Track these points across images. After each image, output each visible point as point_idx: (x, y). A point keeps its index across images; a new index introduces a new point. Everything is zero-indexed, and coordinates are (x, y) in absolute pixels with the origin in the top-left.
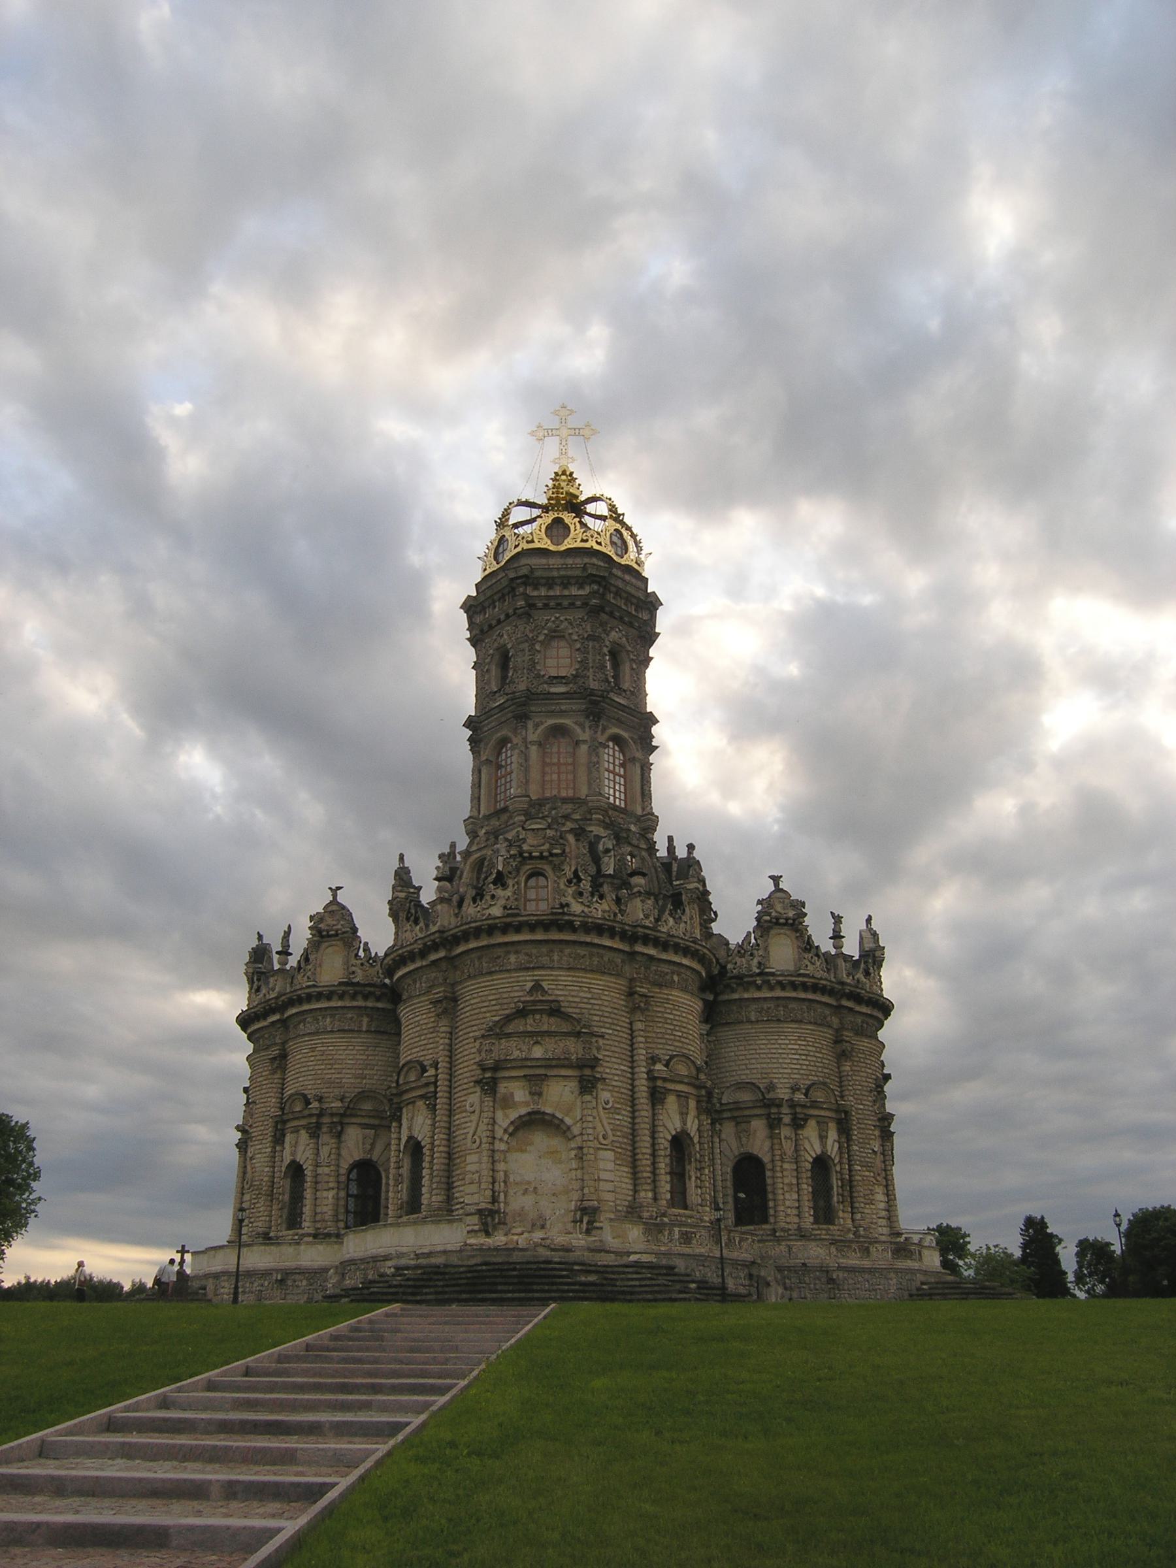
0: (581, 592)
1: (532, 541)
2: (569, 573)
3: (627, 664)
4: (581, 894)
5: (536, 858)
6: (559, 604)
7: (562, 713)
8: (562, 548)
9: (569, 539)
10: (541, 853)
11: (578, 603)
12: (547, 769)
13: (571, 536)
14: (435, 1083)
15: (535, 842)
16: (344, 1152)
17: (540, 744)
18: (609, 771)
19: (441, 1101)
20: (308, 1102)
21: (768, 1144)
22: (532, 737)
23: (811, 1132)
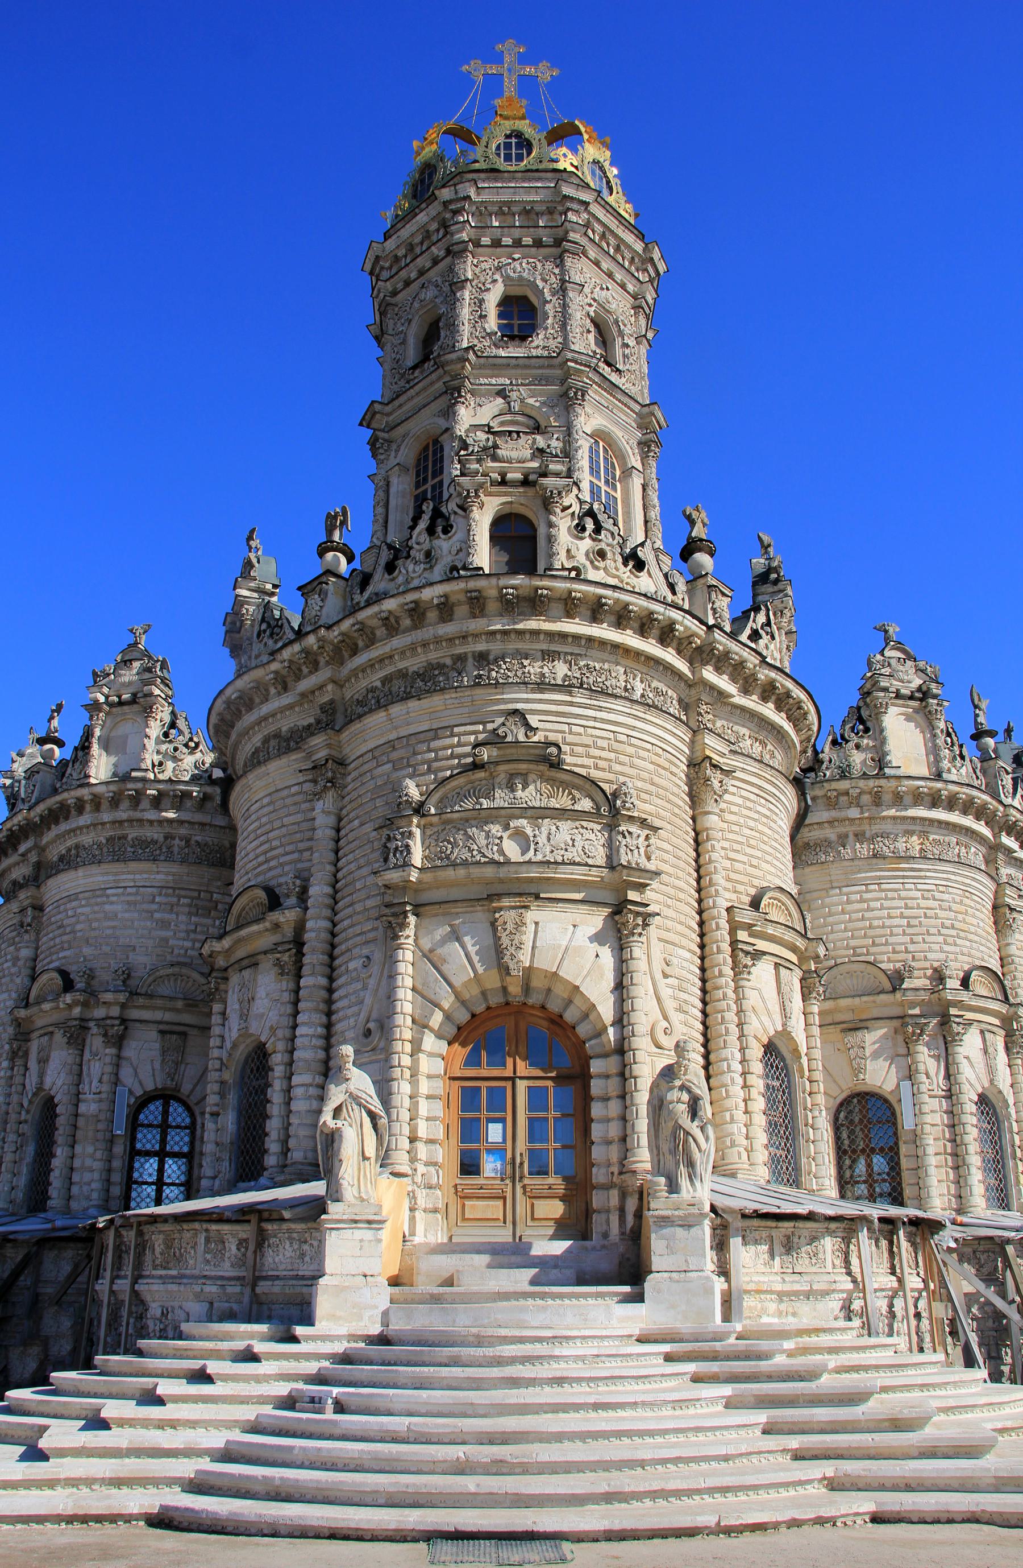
1: (476, 161)
3: (618, 342)
4: (602, 554)
5: (513, 484)
14: (300, 928)
15: (514, 454)
16: (126, 1074)
19: (314, 958)
23: (970, 1046)
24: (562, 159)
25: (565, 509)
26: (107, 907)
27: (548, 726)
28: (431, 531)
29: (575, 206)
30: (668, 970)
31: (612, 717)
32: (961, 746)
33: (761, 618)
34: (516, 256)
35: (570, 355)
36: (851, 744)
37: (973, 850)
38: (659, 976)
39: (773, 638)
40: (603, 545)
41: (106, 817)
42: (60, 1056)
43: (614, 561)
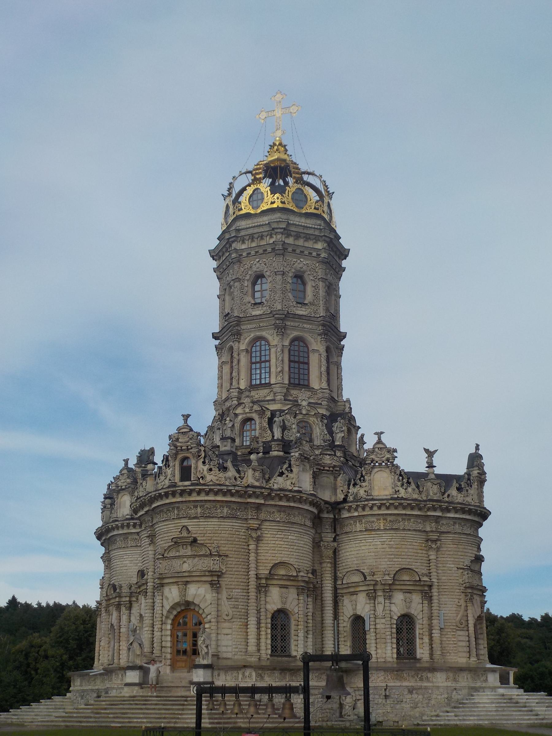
0: (271, 241)
1: (241, 209)
2: (261, 230)
6: (256, 252)
7: (260, 328)
8: (259, 211)
9: (263, 204)
10: (188, 447)
11: (269, 250)
12: (254, 366)
13: (265, 200)
17: (247, 351)
18: (295, 362)
20: (115, 590)
21: (368, 608)
22: (243, 347)
24: (276, 200)
25: (199, 456)
26: (124, 562)
27: (194, 529)
28: (165, 465)
29: (279, 230)
30: (229, 597)
31: (213, 523)
32: (409, 479)
33: (285, 466)
34: (257, 260)
35: (275, 313)
36: (358, 486)
37: (412, 520)
38: (225, 599)
39: (291, 471)
40: (212, 467)
41: (121, 532)
42: (115, 614)
43: (216, 470)
